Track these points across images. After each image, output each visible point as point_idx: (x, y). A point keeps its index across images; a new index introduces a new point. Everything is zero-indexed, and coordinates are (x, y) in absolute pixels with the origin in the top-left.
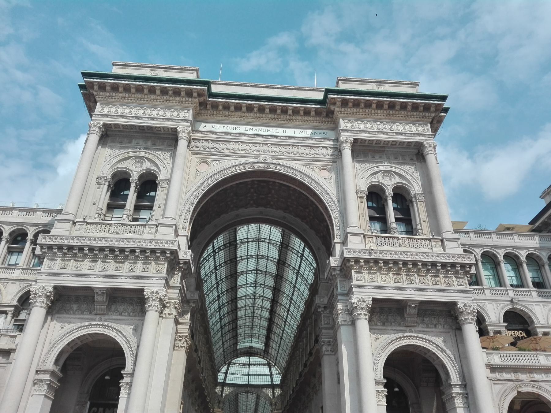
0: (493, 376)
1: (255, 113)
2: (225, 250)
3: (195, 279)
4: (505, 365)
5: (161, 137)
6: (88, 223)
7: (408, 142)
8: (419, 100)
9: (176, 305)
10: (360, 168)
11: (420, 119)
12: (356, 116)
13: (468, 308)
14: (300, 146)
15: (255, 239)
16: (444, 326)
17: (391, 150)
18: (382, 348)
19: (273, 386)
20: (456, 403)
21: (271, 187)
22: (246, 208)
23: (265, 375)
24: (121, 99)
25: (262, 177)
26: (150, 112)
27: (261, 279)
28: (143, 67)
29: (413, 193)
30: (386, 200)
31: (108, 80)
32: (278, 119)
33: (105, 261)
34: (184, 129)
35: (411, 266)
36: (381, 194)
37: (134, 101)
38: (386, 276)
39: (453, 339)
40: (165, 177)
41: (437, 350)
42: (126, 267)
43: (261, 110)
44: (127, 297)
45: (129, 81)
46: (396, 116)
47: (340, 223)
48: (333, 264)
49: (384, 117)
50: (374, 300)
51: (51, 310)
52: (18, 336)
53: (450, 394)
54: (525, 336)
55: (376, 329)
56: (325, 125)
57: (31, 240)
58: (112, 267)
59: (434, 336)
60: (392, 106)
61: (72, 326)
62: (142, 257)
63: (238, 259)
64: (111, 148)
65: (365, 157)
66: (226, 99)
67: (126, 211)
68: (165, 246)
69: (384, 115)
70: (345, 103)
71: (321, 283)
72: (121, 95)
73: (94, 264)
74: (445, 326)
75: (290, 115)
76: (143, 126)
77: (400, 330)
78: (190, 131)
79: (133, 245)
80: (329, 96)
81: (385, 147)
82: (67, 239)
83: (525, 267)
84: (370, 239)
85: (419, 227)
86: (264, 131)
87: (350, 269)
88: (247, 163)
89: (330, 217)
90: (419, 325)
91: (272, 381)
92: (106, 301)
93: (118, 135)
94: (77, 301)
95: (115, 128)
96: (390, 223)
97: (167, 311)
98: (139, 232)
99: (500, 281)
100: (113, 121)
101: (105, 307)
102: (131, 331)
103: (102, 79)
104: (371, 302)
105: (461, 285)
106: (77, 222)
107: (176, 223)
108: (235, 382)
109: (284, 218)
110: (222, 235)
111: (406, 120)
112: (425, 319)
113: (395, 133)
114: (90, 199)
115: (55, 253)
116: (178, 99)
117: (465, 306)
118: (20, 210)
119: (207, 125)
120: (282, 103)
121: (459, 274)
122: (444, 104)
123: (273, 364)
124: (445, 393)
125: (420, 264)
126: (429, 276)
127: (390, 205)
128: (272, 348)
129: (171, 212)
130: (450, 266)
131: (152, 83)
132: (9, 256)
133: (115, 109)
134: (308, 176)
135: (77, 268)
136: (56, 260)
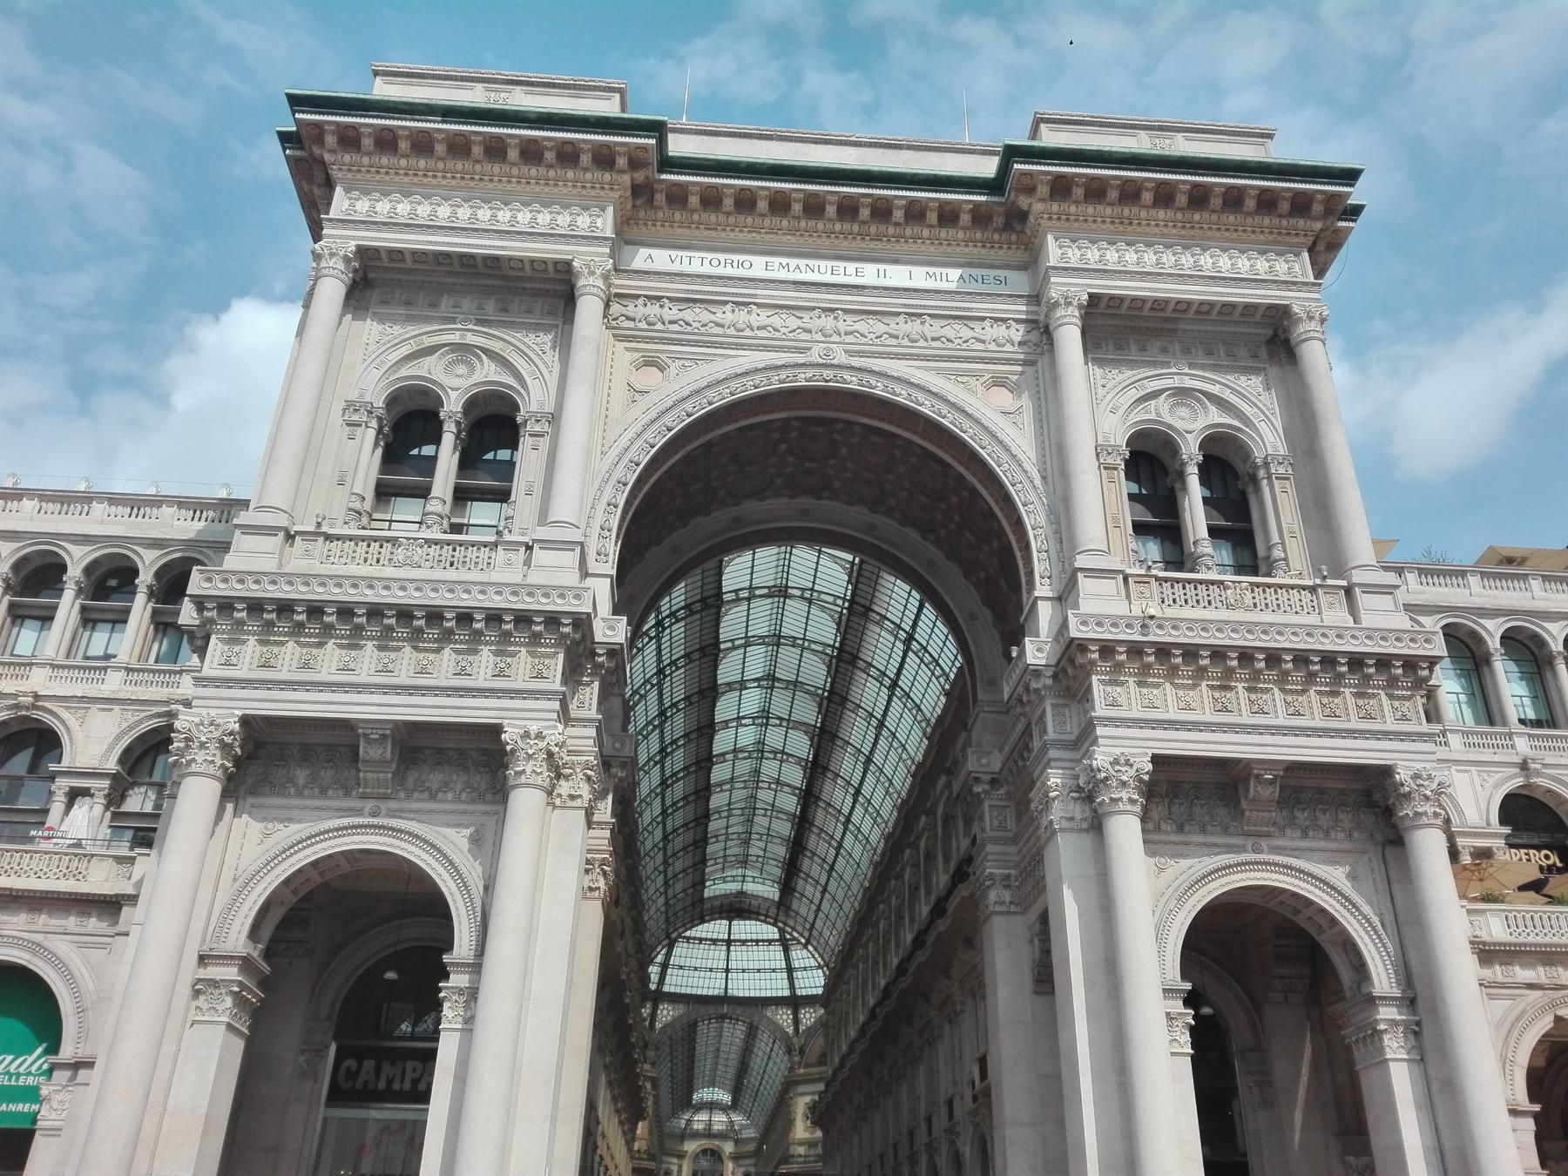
0: (1487, 973)
1: (794, 217)
2: (688, 620)
4: (1520, 945)
5: (524, 289)
6: (329, 538)
7: (1247, 306)
8: (1279, 180)
9: (589, 772)
11: (1280, 238)
12: (1094, 226)
13: (1426, 783)
14: (929, 315)
16: (1350, 836)
18: (1176, 896)
19: (794, 1002)
20: (1387, 1050)
21: (838, 437)
23: (774, 970)
24: (407, 174)
26: (489, 213)
27: (780, 705)
28: (463, 79)
29: (1258, 455)
30: (1181, 476)
33: (386, 646)
34: (591, 263)
35: (1262, 664)
36: (1167, 460)
37: (444, 182)
38: (1191, 693)
39: (1376, 867)
40: (541, 404)
41: (1331, 901)
42: (445, 661)
43: (814, 208)
44: (448, 749)
45: (427, 121)
46: (1210, 229)
48: (1035, 657)
49: (1174, 231)
50: (1156, 759)
51: (232, 785)
52: (139, 859)
53: (1369, 1024)
54: (1559, 864)
55: (1160, 842)
56: (1002, 254)
57: (150, 587)
58: (406, 663)
59: (1324, 862)
60: (1199, 198)
61: (295, 830)
62: (491, 635)
63: (722, 646)
64: (381, 319)
65: (1119, 347)
66: (712, 176)
67: (434, 502)
69: (1174, 226)
71: (982, 715)
72: (403, 162)
73: (354, 653)
74: (1356, 834)
75: (897, 224)
76: (472, 257)
77: (1227, 846)
78: (609, 271)
79: (465, 600)
80: (1016, 166)
81: (1177, 319)
82: (274, 582)
84: (1141, 588)
85: (1277, 553)
87: (1087, 670)
89: (1018, 523)
90: (1282, 830)
91: (792, 986)
93: (400, 281)
94: (307, 760)
95: (391, 260)
96: (1195, 543)
97: (564, 788)
98: (477, 563)
99: (1487, 708)
101: (390, 776)
102: (465, 845)
103: (349, 115)
104: (1150, 765)
105: (1404, 718)
106: (297, 533)
107: (582, 539)
108: (689, 991)
109: (871, 528)
112: (1298, 814)
113: (1210, 277)
115: (241, 623)
116: (570, 174)
117: (1416, 776)
119: (655, 252)
120: (876, 187)
121: (1398, 688)
123: (803, 941)
126: (1312, 692)
127: (1194, 495)
128: (803, 895)
129: (566, 505)
130: (1375, 664)
131: (496, 126)
132: (87, 634)
133: (388, 206)
134: (953, 405)
135: (306, 666)
136: (244, 642)
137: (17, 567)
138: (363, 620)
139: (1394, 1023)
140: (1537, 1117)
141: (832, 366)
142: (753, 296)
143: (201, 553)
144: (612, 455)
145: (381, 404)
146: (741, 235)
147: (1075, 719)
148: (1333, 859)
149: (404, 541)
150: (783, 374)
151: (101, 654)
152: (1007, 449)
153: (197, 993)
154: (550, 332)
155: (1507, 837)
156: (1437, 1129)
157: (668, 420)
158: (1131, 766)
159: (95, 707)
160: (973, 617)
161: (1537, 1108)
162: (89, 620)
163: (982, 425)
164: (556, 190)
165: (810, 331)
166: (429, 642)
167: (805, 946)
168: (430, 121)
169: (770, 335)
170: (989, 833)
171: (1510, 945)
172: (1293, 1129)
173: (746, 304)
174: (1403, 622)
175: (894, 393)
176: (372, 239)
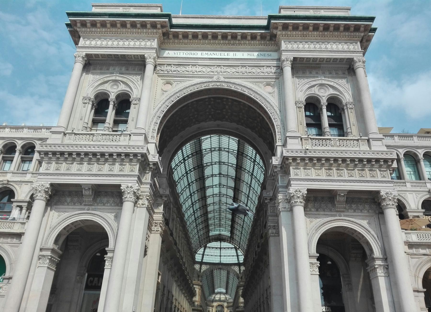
0: (411, 251)
3: (167, 179)
4: (421, 243)
5: (133, 63)
6: (75, 134)
9: (147, 197)
10: (299, 83)
11: (351, 39)
12: (296, 38)
14: (248, 66)
17: (326, 66)
18: (315, 229)
19: (239, 264)
20: (378, 273)
21: (225, 103)
23: (233, 256)
24: (100, 33)
28: (117, 6)
29: (344, 102)
30: (321, 109)
31: (88, 17)
35: (341, 162)
37: (110, 35)
39: (376, 221)
40: (137, 96)
42: (106, 168)
43: (215, 37)
45: (104, 18)
46: (330, 37)
47: (282, 129)
49: (319, 38)
50: (308, 190)
51: (50, 203)
52: (26, 223)
53: (373, 266)
56: (270, 47)
58: (95, 168)
59: (360, 219)
61: (67, 214)
64: (93, 74)
65: (304, 73)
66: (185, 29)
67: (107, 124)
69: (319, 36)
71: (268, 181)
72: (99, 30)
73: (81, 166)
74: (370, 211)
75: (239, 40)
76: (117, 55)
78: (155, 57)
79: (111, 150)
81: (321, 64)
82: (59, 147)
84: (306, 141)
85: (349, 130)
87: (288, 166)
88: (203, 83)
89: (273, 125)
90: (348, 210)
92: (92, 195)
93: (98, 63)
94: (70, 195)
95: (96, 57)
97: (140, 202)
100: (93, 52)
101: (92, 199)
102: (113, 218)
103: (83, 17)
104: (306, 192)
105: (384, 177)
106: (67, 133)
108: (210, 262)
109: (237, 129)
110: (189, 144)
111: (339, 40)
112: (353, 205)
113: (329, 51)
114: (78, 116)
115: (51, 158)
116: (145, 30)
117: (387, 194)
118: (29, 128)
119: (170, 52)
120: (232, 30)
121: (382, 168)
123: (238, 247)
124: (369, 265)
125: (348, 160)
126: (356, 170)
127: (325, 114)
128: (236, 235)
130: (375, 161)
131: (123, 18)
132: (23, 164)
134: (254, 91)
135: (68, 169)
136: (52, 163)
137: (4, 147)
138: (83, 156)
139: (380, 265)
140: (425, 293)
141: (219, 82)
142: (197, 63)
144: (156, 109)
145: (93, 97)
150: (205, 85)
151: (26, 169)
152: (269, 103)
153: (39, 259)
154: (140, 75)
155: (424, 213)
156: (392, 296)
157: (172, 99)
158: (301, 192)
159: (23, 184)
160: (266, 153)
161: (425, 290)
162: (23, 160)
163: (263, 97)
164: (141, 35)
165: (213, 72)
166: (102, 162)
168: (105, 18)
171: (418, 243)
172: (357, 297)
173: (195, 65)
174: (385, 149)
176: (90, 52)
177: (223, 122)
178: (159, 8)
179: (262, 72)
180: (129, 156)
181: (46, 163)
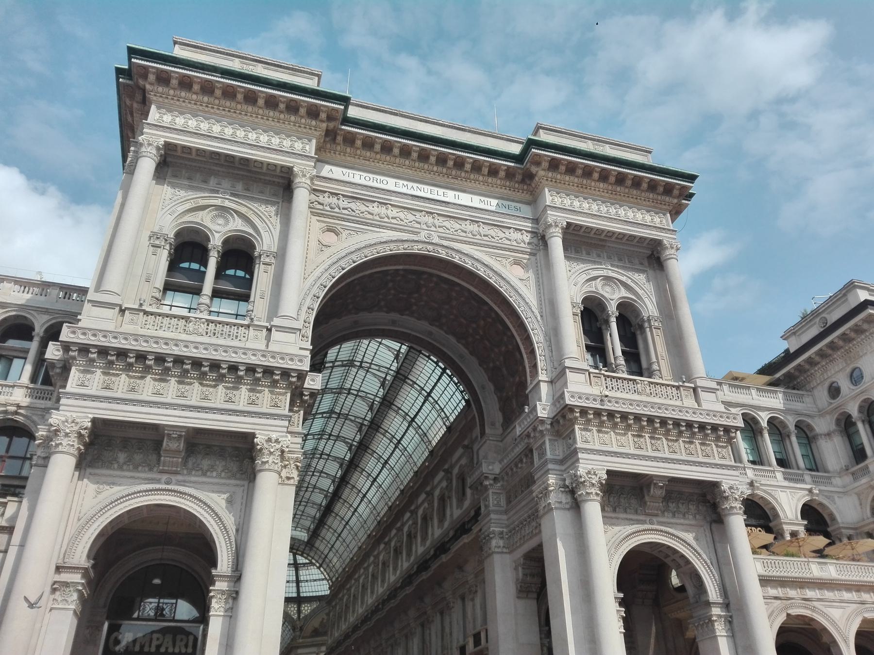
5: (260, 179)
6: (146, 313)
14: (482, 222)
15: (345, 363)
17: (616, 246)
20: (717, 630)
22: (371, 313)
25: (420, 266)
28: (227, 54)
29: (645, 315)
30: (607, 322)
31: (175, 67)
32: (448, 175)
33: (183, 381)
35: (658, 425)
36: (598, 313)
38: (624, 438)
39: (708, 534)
40: (270, 247)
43: (424, 156)
44: (214, 446)
45: (212, 75)
47: (547, 351)
49: (607, 195)
50: (609, 472)
53: (706, 617)
56: (519, 195)
58: (195, 392)
59: (683, 530)
61: (116, 491)
64: (173, 186)
65: (577, 252)
67: (205, 297)
68: (287, 364)
70: (554, 165)
71: (488, 442)
72: (194, 97)
73: (163, 384)
74: (697, 516)
75: (467, 172)
76: (233, 157)
81: (606, 240)
82: (115, 338)
83: (766, 435)
84: (596, 380)
85: (655, 367)
86: (426, 191)
87: (572, 422)
89: (528, 339)
95: (183, 152)
100: (181, 140)
101: (180, 460)
102: (223, 504)
103: (165, 65)
104: (605, 477)
105: (723, 457)
106: (126, 308)
109: (430, 334)
111: (638, 204)
112: (670, 504)
115: (93, 360)
116: (293, 118)
119: (334, 168)
120: (458, 150)
122: (692, 187)
128: (324, 538)
134: (495, 272)
136: (93, 372)
138: (171, 365)
139: (720, 616)
141: (432, 243)
143: (29, 313)
144: (311, 280)
146: (382, 165)
147: (561, 449)
148: (687, 528)
149: (193, 319)
152: (524, 299)
154: (274, 205)
157: (342, 263)
158: (596, 475)
165: (420, 223)
166: (209, 381)
167: (319, 568)
168: (214, 76)
169: (399, 223)
170: (492, 508)
173: (386, 204)
174: (721, 408)
175: (465, 262)
176: (173, 138)
177: (404, 317)
178: (317, 78)
179: (507, 239)
180: (164, 361)
181: (79, 371)
